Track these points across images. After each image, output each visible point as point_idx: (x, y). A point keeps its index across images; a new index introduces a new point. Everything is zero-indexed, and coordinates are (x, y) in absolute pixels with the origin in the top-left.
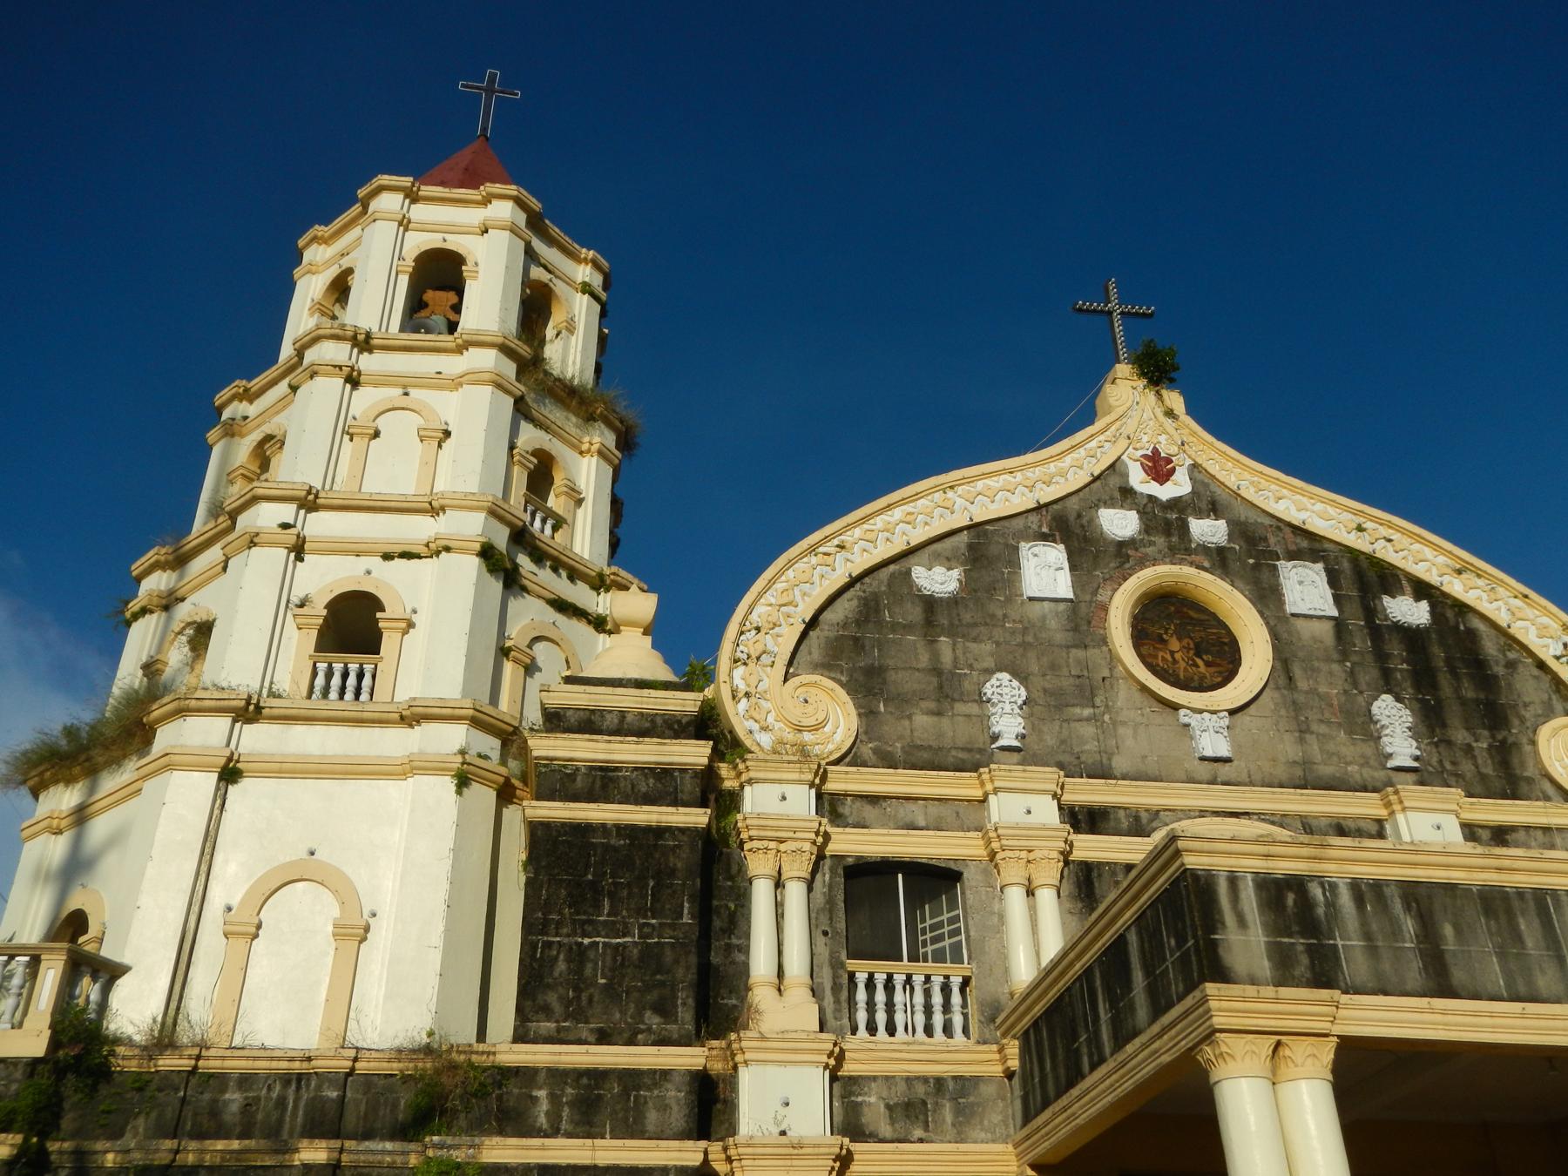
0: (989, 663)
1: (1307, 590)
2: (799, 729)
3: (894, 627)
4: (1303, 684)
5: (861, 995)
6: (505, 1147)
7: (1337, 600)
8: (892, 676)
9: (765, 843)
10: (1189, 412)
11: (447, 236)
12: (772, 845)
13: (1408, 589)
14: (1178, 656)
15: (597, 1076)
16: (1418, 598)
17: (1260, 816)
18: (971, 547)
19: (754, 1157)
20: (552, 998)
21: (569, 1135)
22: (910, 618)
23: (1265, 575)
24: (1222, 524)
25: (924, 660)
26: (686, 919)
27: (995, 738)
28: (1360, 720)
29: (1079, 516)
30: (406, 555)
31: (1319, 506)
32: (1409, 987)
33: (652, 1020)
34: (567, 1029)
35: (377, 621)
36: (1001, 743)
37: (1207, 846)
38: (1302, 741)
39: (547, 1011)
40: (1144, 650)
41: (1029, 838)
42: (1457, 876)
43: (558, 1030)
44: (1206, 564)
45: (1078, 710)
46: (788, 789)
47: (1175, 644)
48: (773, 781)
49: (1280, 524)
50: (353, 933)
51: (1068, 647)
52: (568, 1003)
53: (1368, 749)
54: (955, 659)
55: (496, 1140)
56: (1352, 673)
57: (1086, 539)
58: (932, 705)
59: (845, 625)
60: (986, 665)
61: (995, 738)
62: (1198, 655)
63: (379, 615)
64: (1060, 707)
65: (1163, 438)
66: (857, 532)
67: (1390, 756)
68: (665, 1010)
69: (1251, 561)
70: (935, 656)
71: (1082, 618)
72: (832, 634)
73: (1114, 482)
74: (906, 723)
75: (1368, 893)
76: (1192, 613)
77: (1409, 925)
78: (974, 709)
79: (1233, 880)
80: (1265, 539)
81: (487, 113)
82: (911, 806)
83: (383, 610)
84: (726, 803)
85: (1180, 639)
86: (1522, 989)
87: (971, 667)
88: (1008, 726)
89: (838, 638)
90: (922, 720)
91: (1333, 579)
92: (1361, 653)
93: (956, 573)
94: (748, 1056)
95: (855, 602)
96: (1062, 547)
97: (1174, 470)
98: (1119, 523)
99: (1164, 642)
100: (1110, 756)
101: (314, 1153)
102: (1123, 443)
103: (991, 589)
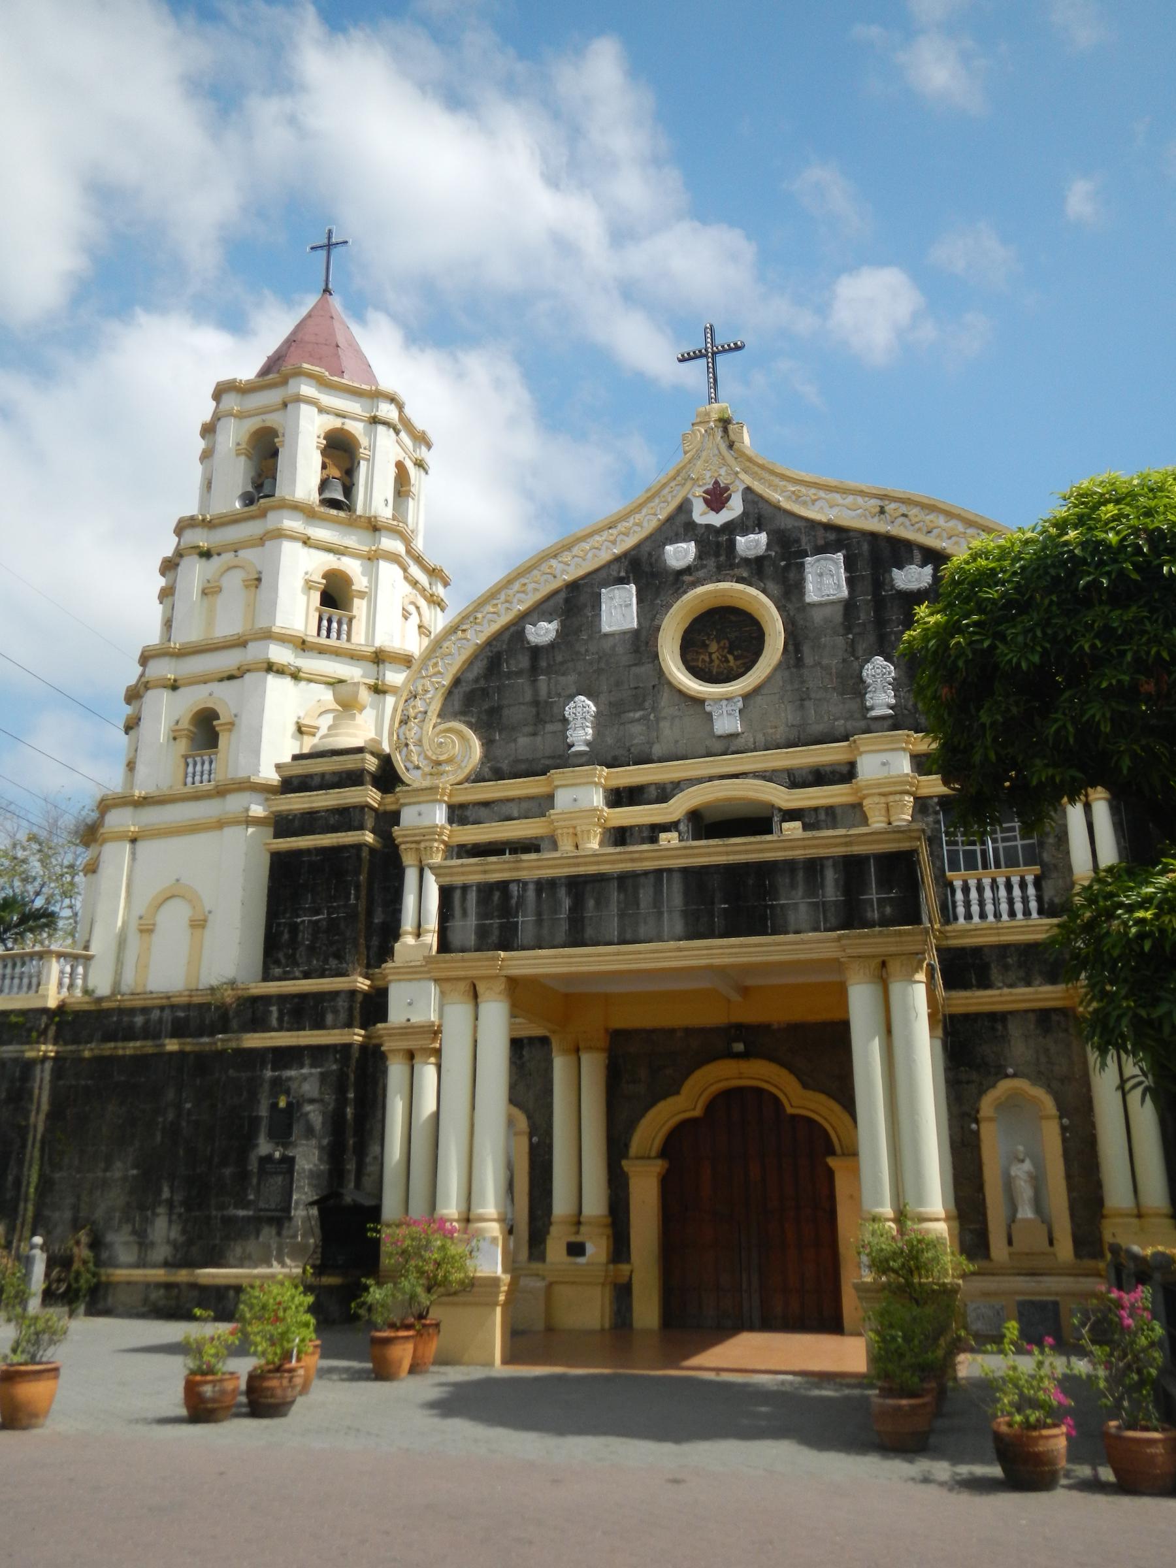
0: (573, 690)
1: (826, 580)
2: (438, 763)
3: (509, 675)
4: (809, 660)
6: (253, 1039)
7: (850, 582)
8: (506, 712)
9: (408, 845)
11: (264, 417)
12: (413, 846)
13: (917, 556)
14: (714, 656)
15: (303, 997)
16: (923, 565)
17: (756, 775)
18: (567, 601)
19: (390, 1035)
20: (281, 956)
21: (289, 1030)
22: (521, 666)
23: (792, 575)
24: (763, 537)
25: (528, 696)
26: (352, 901)
28: (851, 682)
29: (650, 554)
30: (231, 677)
32: (556, 943)
33: (333, 963)
34: (288, 972)
35: (213, 728)
36: (573, 749)
37: (447, 871)
38: (802, 707)
39: (277, 963)
40: (689, 657)
41: (571, 819)
42: (605, 868)
43: (285, 972)
44: (745, 575)
45: (631, 715)
46: (423, 808)
48: (414, 803)
49: (813, 524)
50: (199, 924)
51: (630, 666)
52: (287, 957)
53: (854, 705)
54: (549, 693)
55: (249, 1035)
56: (852, 645)
57: (654, 575)
58: (530, 729)
59: (477, 680)
60: (569, 692)
62: (730, 652)
63: (215, 723)
64: (619, 715)
65: (723, 471)
67: (872, 708)
68: (339, 956)
69: (783, 563)
70: (536, 692)
71: (642, 643)
72: (468, 689)
73: (682, 518)
74: (513, 745)
75: (546, 886)
76: (733, 618)
77: (566, 903)
78: (558, 726)
79: (465, 888)
80: (798, 541)
82: (511, 804)
83: (218, 718)
84: (388, 820)
85: (718, 642)
86: (628, 936)
87: (559, 695)
88: (581, 735)
89: (473, 691)
90: (523, 741)
91: (849, 566)
92: (864, 624)
94: (390, 978)
95: (485, 662)
97: (730, 496)
98: (681, 554)
99: (706, 646)
100: (651, 744)
101: (172, 1045)
102: (689, 484)
103: (579, 630)
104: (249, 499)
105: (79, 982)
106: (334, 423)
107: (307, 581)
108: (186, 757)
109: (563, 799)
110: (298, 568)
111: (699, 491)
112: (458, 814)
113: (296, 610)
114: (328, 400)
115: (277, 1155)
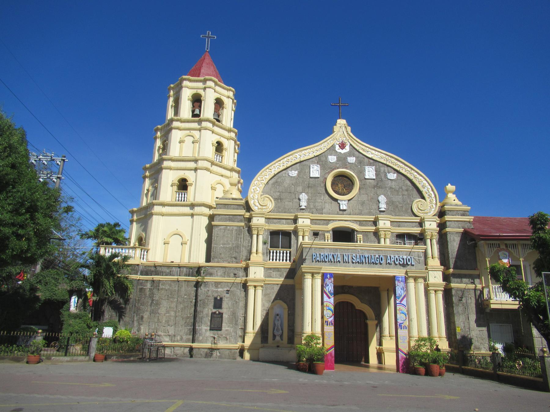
1: (370, 173)
5: (271, 254)
10: (352, 132)
16: (394, 173)
24: (354, 158)
27: (300, 206)
31: (377, 153)
47: (340, 185)
61: (300, 206)
66: (277, 164)
81: (208, 44)
93: (296, 172)
96: (319, 166)
98: (332, 159)
99: (337, 185)
104: (194, 115)
105: (145, 257)
106: (218, 96)
107: (212, 144)
108: (176, 192)
109: (300, 221)
110: (209, 139)
111: (338, 143)
112: (269, 220)
113: (209, 152)
114: (218, 88)
115: (217, 312)
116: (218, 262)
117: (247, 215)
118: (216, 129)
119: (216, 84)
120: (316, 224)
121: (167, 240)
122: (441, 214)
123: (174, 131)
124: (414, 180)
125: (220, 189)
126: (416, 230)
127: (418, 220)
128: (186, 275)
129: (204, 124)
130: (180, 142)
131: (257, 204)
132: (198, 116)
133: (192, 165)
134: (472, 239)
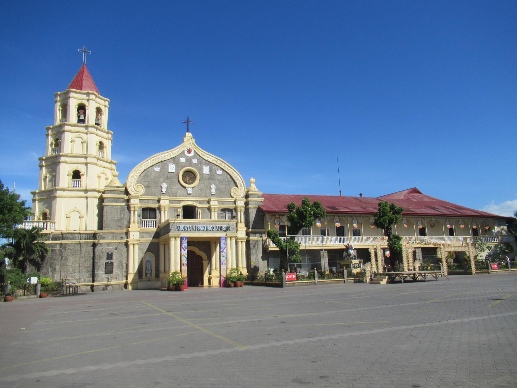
1: (206, 170)
47: (187, 178)
98: (183, 160)
106: (98, 105)
107: (97, 144)
109: (162, 202)
110: (94, 140)
113: (94, 150)
116: (108, 230)
117: (126, 197)
118: (99, 132)
119: (96, 96)
120: (172, 203)
121: (68, 216)
122: (247, 196)
123: (66, 134)
124: (232, 175)
125: (103, 177)
126: (232, 206)
127: (233, 200)
128: (85, 239)
129: (90, 129)
130: (71, 142)
131: (133, 190)
132: (83, 121)
133: (83, 160)
134: (262, 212)
